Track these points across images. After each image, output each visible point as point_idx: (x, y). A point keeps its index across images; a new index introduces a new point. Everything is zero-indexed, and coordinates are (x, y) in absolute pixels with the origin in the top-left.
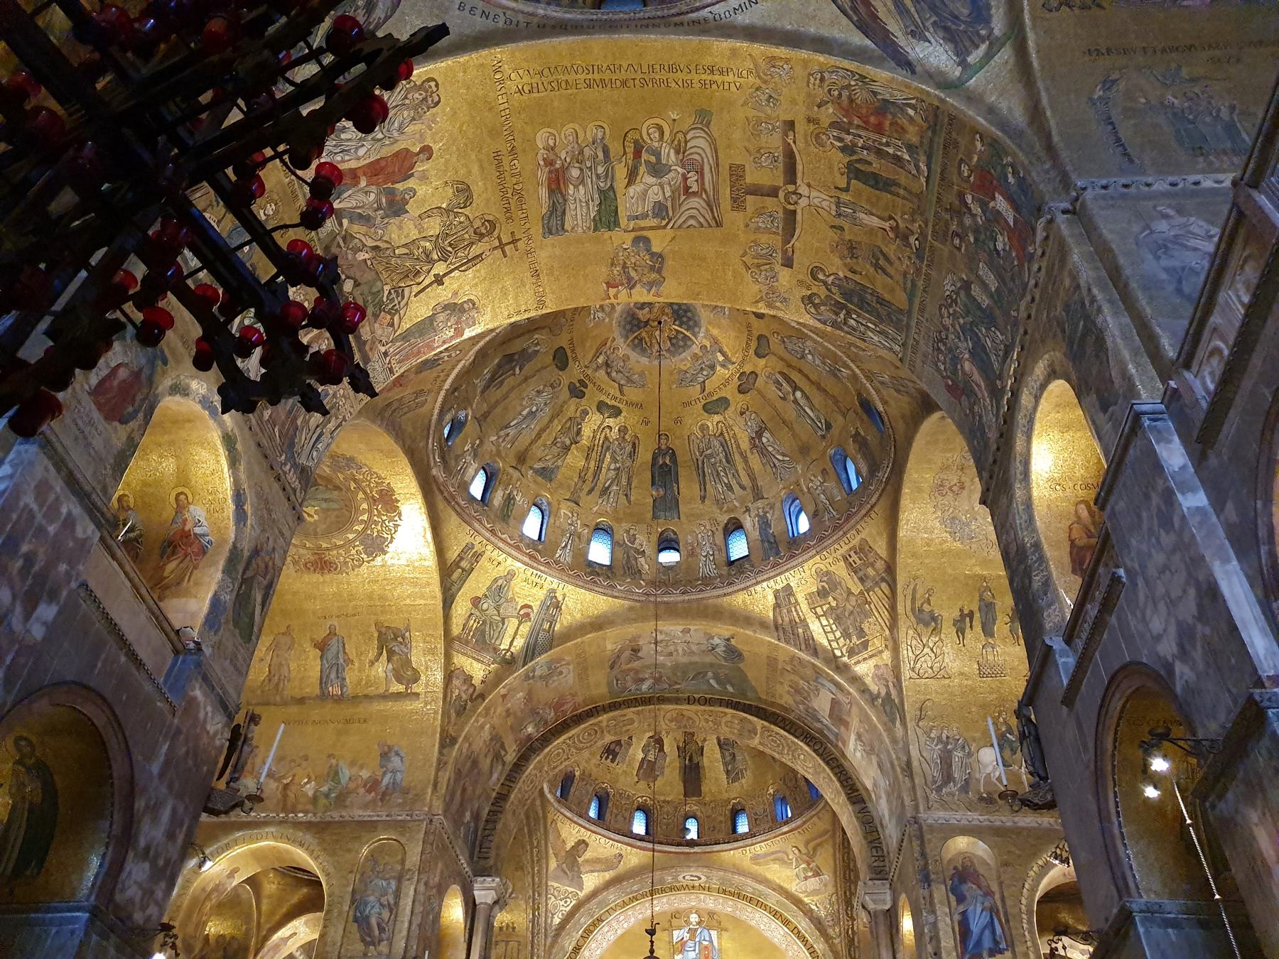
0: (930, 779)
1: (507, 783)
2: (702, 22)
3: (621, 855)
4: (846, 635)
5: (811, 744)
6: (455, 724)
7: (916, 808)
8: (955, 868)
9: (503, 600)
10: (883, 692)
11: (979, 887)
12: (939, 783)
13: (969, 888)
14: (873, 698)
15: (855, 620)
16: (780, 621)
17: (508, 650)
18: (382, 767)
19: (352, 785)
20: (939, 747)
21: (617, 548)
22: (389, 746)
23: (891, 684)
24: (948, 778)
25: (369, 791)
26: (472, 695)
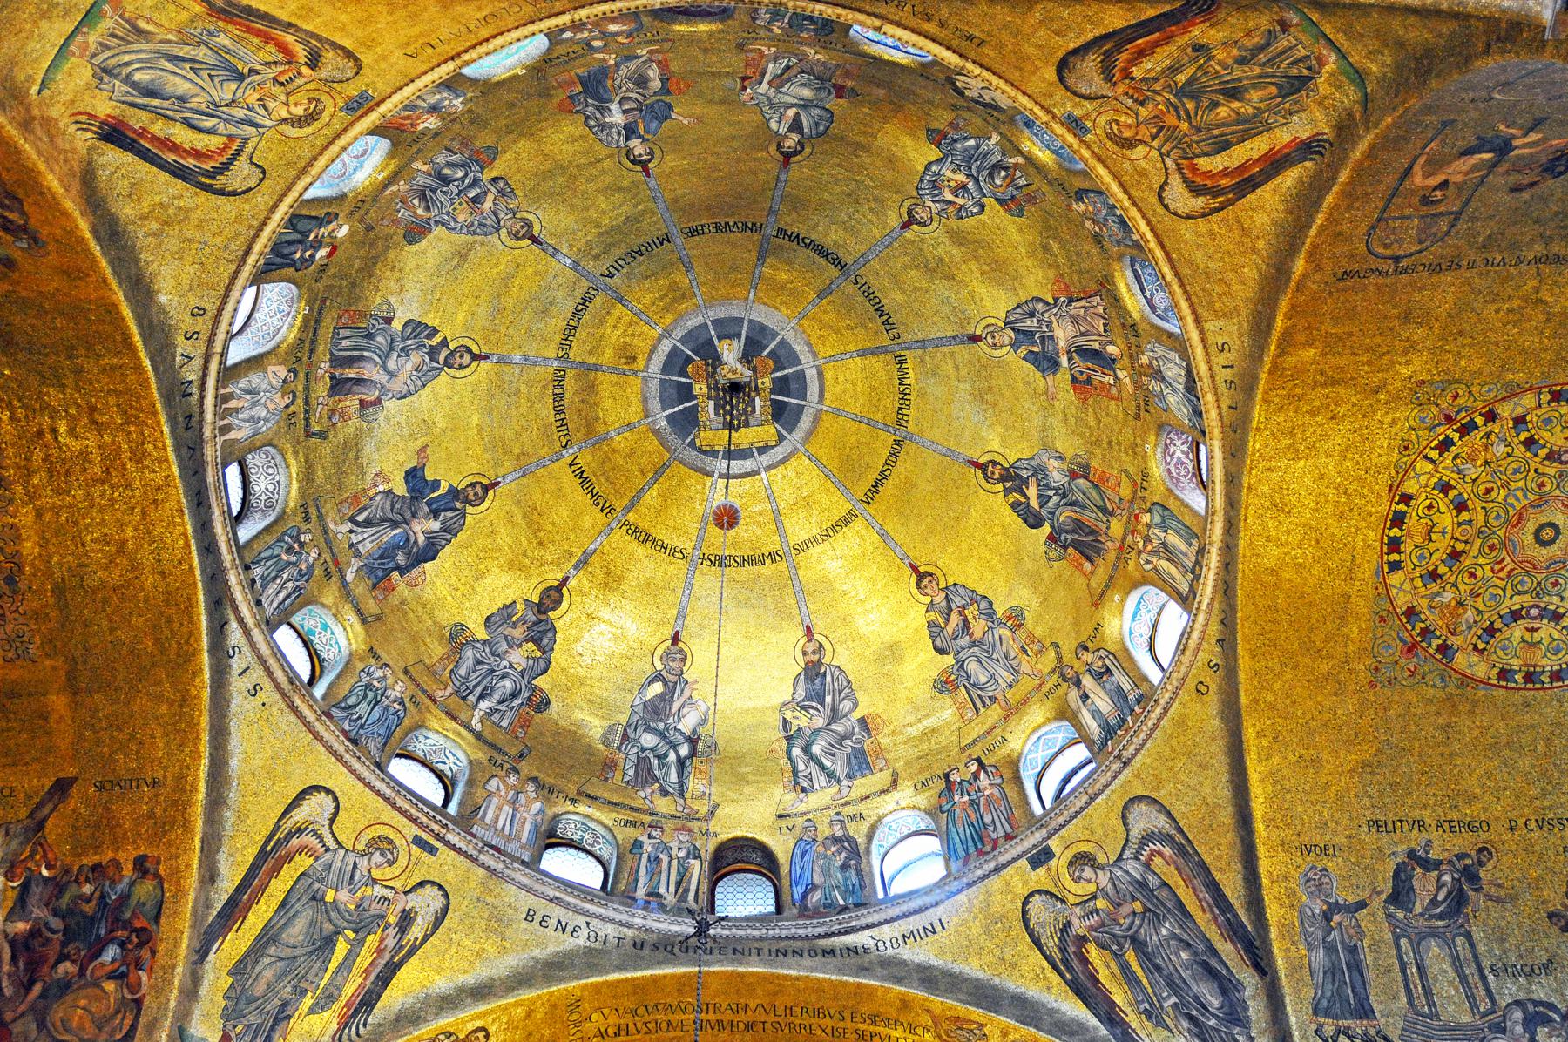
2: (861, 950)
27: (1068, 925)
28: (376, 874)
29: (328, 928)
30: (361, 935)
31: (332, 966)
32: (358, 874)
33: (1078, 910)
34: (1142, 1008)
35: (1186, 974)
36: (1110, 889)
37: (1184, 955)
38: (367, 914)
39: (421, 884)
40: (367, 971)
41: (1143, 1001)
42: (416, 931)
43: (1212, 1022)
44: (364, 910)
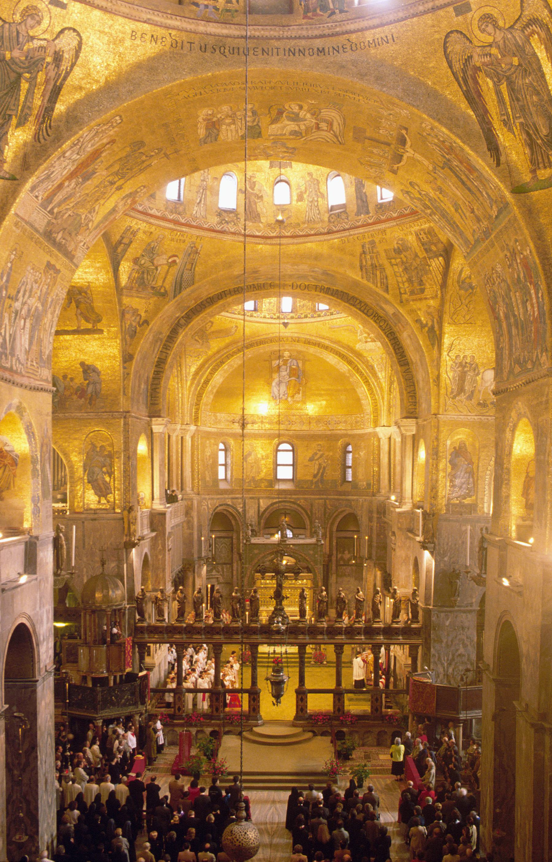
0: (449, 390)
1: (164, 350)
3: (236, 327)
4: (410, 280)
5: (377, 321)
6: (130, 345)
7: (439, 407)
8: (455, 448)
9: (155, 256)
10: (430, 324)
11: (466, 460)
12: (455, 393)
13: (461, 461)
14: (423, 326)
15: (418, 273)
16: (364, 263)
17: (161, 287)
18: (85, 380)
19: (67, 393)
20: (460, 369)
21: (240, 195)
22: (87, 365)
23: (435, 320)
24: (461, 390)
25: (80, 397)
26: (139, 322)
27: (471, 57)
28: (31, 34)
29: (13, 76)
30: (34, 75)
31: (22, 98)
32: (21, 36)
33: (478, 50)
34: (503, 118)
35: (533, 109)
36: (501, 43)
37: (535, 98)
38: (33, 60)
39: (62, 31)
40: (43, 95)
41: (504, 114)
42: (65, 66)
43: (539, 142)
44: (31, 58)
